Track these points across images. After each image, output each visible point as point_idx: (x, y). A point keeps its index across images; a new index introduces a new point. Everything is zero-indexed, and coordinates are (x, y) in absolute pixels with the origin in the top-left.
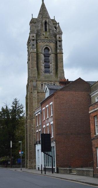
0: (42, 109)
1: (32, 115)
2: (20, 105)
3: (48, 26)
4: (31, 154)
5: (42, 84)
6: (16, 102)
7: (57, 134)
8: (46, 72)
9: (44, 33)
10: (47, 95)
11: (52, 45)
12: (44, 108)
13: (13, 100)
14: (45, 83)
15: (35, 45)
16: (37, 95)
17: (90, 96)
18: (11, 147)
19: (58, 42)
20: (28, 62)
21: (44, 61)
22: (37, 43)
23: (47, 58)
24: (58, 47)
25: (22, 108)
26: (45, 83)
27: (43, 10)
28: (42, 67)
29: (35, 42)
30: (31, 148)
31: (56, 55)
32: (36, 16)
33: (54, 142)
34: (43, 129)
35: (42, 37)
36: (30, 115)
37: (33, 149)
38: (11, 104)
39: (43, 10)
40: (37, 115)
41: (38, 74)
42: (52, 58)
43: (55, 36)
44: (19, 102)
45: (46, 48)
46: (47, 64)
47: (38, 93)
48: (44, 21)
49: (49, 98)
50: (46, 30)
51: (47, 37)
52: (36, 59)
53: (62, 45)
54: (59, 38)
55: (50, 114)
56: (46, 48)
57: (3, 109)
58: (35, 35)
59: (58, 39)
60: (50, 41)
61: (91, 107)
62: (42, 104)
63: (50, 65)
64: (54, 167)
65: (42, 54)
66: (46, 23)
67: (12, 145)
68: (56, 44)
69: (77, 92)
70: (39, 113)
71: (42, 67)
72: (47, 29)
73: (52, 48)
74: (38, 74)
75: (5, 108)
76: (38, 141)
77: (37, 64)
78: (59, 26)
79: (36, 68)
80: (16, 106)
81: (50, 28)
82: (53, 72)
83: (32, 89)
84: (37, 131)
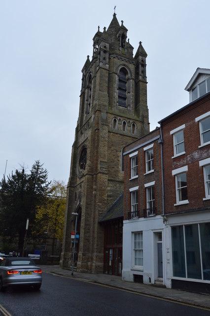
1: (97, 167)
2: (43, 171)
4: (88, 241)
5: (115, 120)
6: (38, 166)
13: (34, 163)
14: (120, 119)
15: (108, 60)
19: (140, 66)
22: (110, 59)
24: (140, 73)
25: (45, 176)
26: (120, 119)
28: (116, 94)
29: (107, 55)
30: (89, 229)
32: (102, 31)
46: (122, 92)
52: (107, 79)
54: (142, 60)
57: (17, 172)
65: (116, 76)
67: (29, 226)
71: (116, 94)
73: (132, 72)
74: (110, 104)
77: (109, 87)
78: (141, 47)
82: (131, 106)
83: (98, 123)
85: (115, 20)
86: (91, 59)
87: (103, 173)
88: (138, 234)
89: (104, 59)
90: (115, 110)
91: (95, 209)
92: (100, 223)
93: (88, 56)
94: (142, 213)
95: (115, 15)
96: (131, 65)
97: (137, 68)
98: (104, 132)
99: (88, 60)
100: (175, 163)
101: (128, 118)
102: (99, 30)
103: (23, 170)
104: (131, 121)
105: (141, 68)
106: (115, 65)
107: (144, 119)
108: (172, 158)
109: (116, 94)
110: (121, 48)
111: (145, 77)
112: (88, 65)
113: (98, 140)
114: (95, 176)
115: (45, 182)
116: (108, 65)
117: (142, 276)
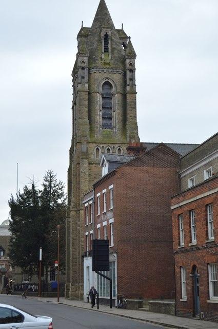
0: (95, 195)
2: (58, 183)
3: (110, 42)
4: (76, 273)
6: (51, 177)
7: (118, 242)
8: (105, 126)
9: (103, 56)
10: (105, 171)
11: (117, 78)
12: (99, 195)
13: (45, 174)
14: (103, 147)
15: (87, 78)
16: (87, 169)
17: (180, 175)
18: (41, 259)
19: (128, 72)
20: (73, 107)
21: (101, 107)
22: (89, 73)
23: (107, 101)
24: (128, 82)
26: (103, 147)
27: (102, 13)
29: (86, 71)
31: (124, 96)
32: (89, 24)
33: (115, 255)
34: (96, 230)
35: (99, 63)
36: (76, 204)
37: (79, 264)
38: (42, 181)
39: (102, 13)
40: (86, 205)
42: (117, 102)
43: (123, 61)
45: (107, 83)
46: (106, 111)
47: (89, 164)
48: (103, 33)
49: (107, 177)
50: (106, 50)
51: (109, 64)
53: (135, 78)
55: (108, 206)
56: (107, 83)
57: (26, 189)
58: (86, 59)
59: (128, 66)
60: (114, 70)
61: (174, 199)
62: (95, 186)
63: (114, 114)
64: (113, 298)
65: (98, 95)
66: (106, 36)
68: (125, 75)
69: (156, 169)
70: (91, 202)
71: (98, 117)
72: (108, 49)
75: (30, 188)
76: (88, 250)
77: (90, 111)
79: (87, 119)
80: (50, 184)
81: (114, 46)
82: (117, 127)
84: (87, 233)
90: (98, 136)
96: (115, 75)
101: (112, 144)
102: (82, 26)
103: (33, 186)
104: (116, 146)
105: (128, 74)
109: (98, 117)
111: (133, 86)
113: (79, 174)
116: (87, 85)
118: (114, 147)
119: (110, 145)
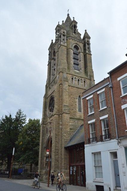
1: (62, 110)
5: (72, 78)
6: (20, 113)
13: (17, 111)
14: (75, 78)
15: (66, 40)
19: (87, 44)
22: (67, 40)
24: (87, 49)
25: (25, 119)
28: (72, 61)
29: (65, 37)
31: (85, 56)
32: (61, 24)
36: (58, 110)
41: (69, 68)
44: (23, 113)
46: (76, 61)
57: (6, 117)
59: (86, 41)
65: (72, 50)
67: (14, 153)
74: (69, 68)
75: (8, 116)
76: (91, 137)
78: (86, 33)
79: (66, 61)
80: (20, 116)
82: (82, 69)
85: (68, 17)
86: (54, 42)
87: (66, 113)
88: (96, 154)
89: (64, 40)
90: (72, 72)
91: (61, 138)
92: (66, 148)
93: (52, 40)
94: (99, 139)
95: (68, 15)
97: (85, 46)
98: (66, 86)
99: (52, 42)
100: (123, 100)
102: (59, 24)
103: (10, 116)
104: (83, 79)
106: (70, 45)
107: (91, 77)
108: (121, 96)
110: (74, 34)
111: (90, 51)
112: (52, 46)
113: (62, 91)
114: (60, 115)
115: (25, 123)
117: (102, 187)
118: (81, 79)
119: (80, 78)
